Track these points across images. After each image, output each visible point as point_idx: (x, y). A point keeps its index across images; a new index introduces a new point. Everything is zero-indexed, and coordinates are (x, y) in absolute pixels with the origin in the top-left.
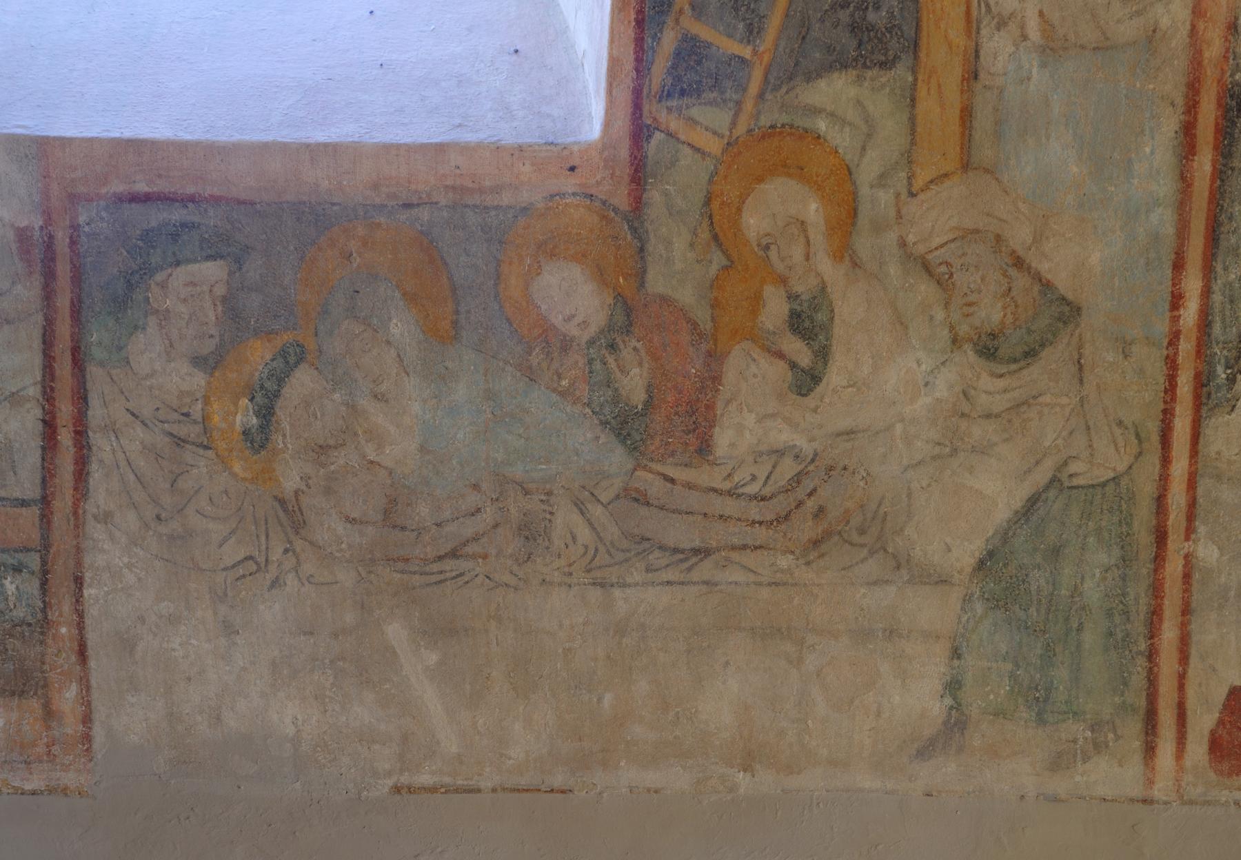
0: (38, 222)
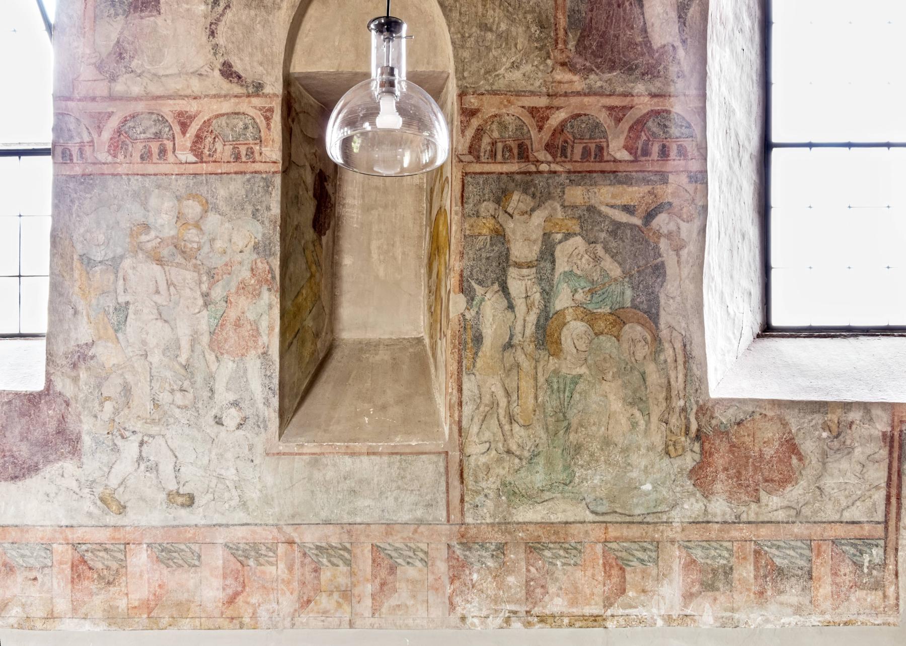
0: (889, 429)
